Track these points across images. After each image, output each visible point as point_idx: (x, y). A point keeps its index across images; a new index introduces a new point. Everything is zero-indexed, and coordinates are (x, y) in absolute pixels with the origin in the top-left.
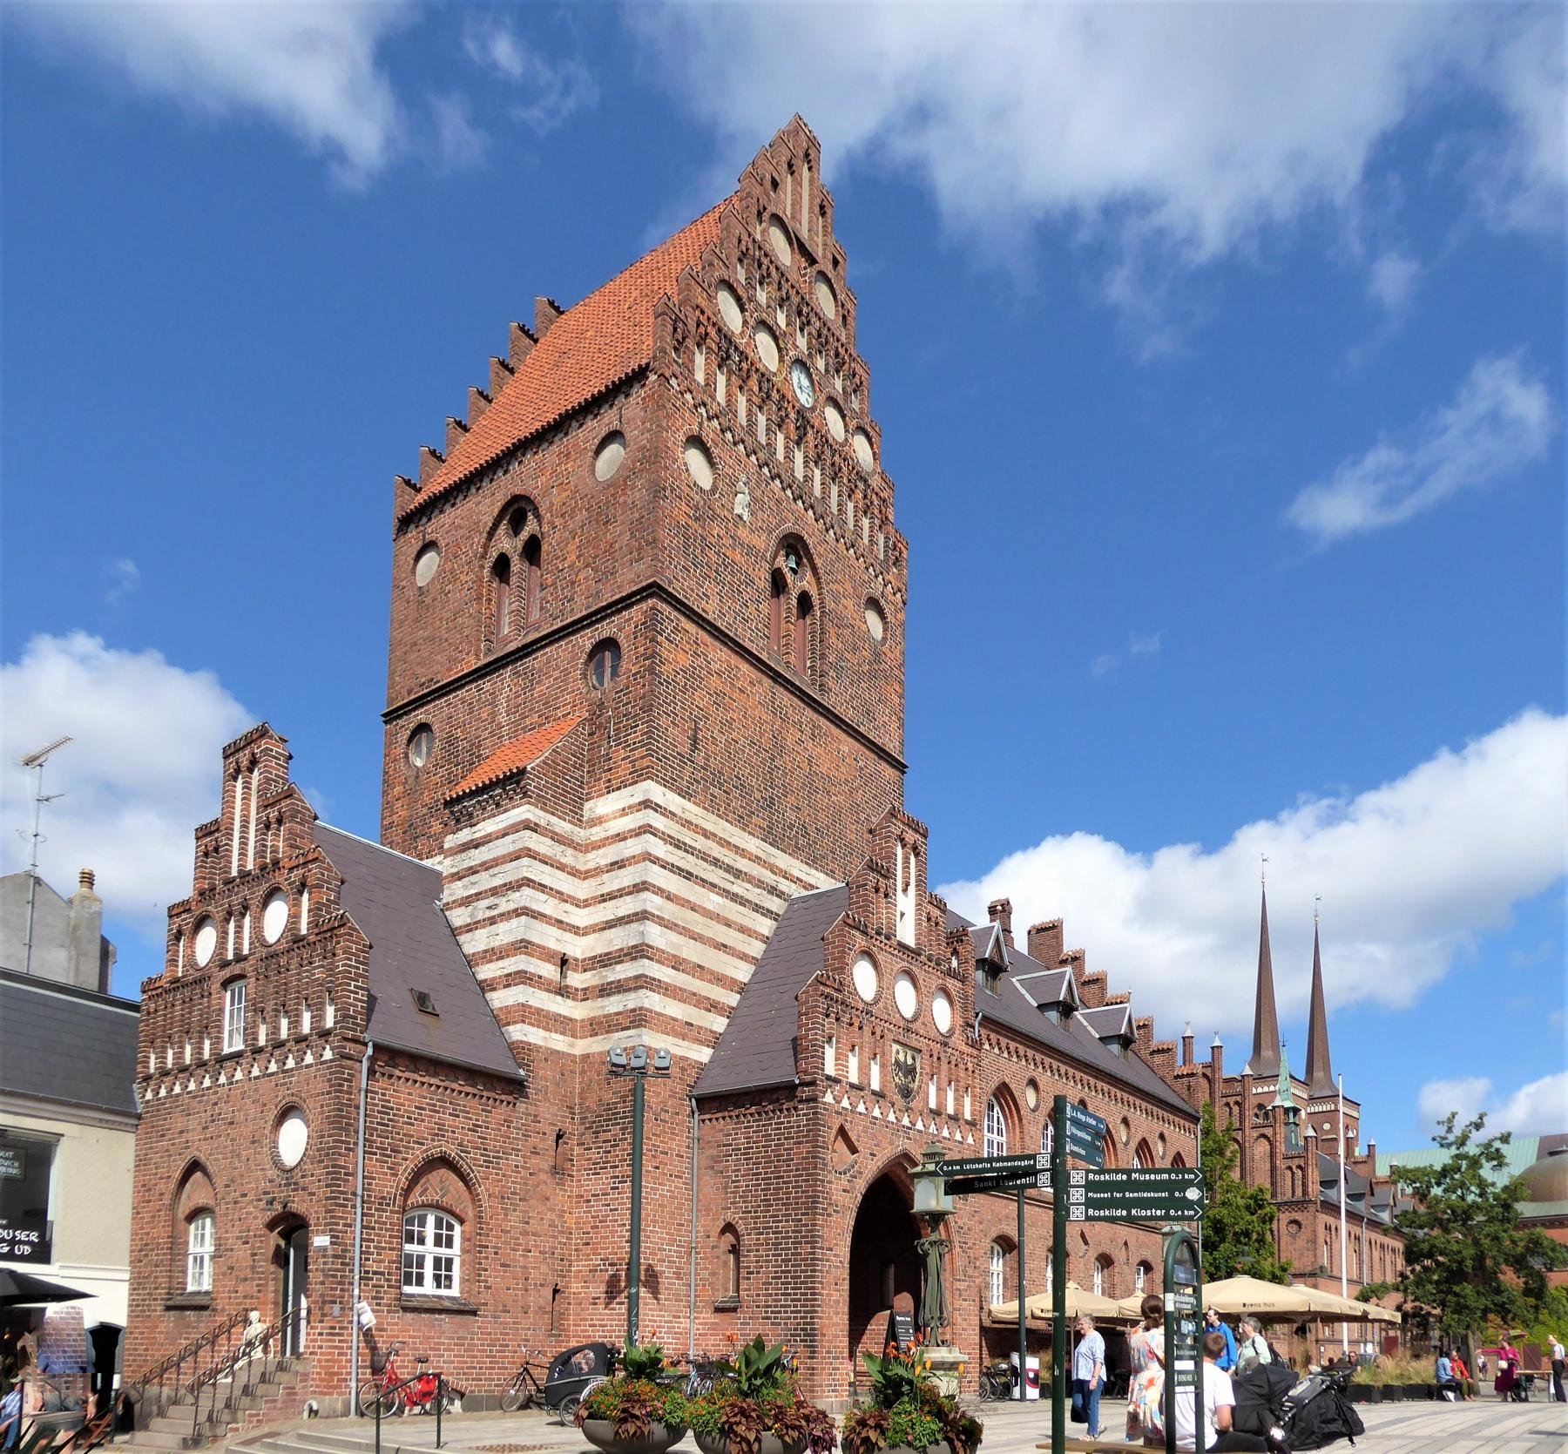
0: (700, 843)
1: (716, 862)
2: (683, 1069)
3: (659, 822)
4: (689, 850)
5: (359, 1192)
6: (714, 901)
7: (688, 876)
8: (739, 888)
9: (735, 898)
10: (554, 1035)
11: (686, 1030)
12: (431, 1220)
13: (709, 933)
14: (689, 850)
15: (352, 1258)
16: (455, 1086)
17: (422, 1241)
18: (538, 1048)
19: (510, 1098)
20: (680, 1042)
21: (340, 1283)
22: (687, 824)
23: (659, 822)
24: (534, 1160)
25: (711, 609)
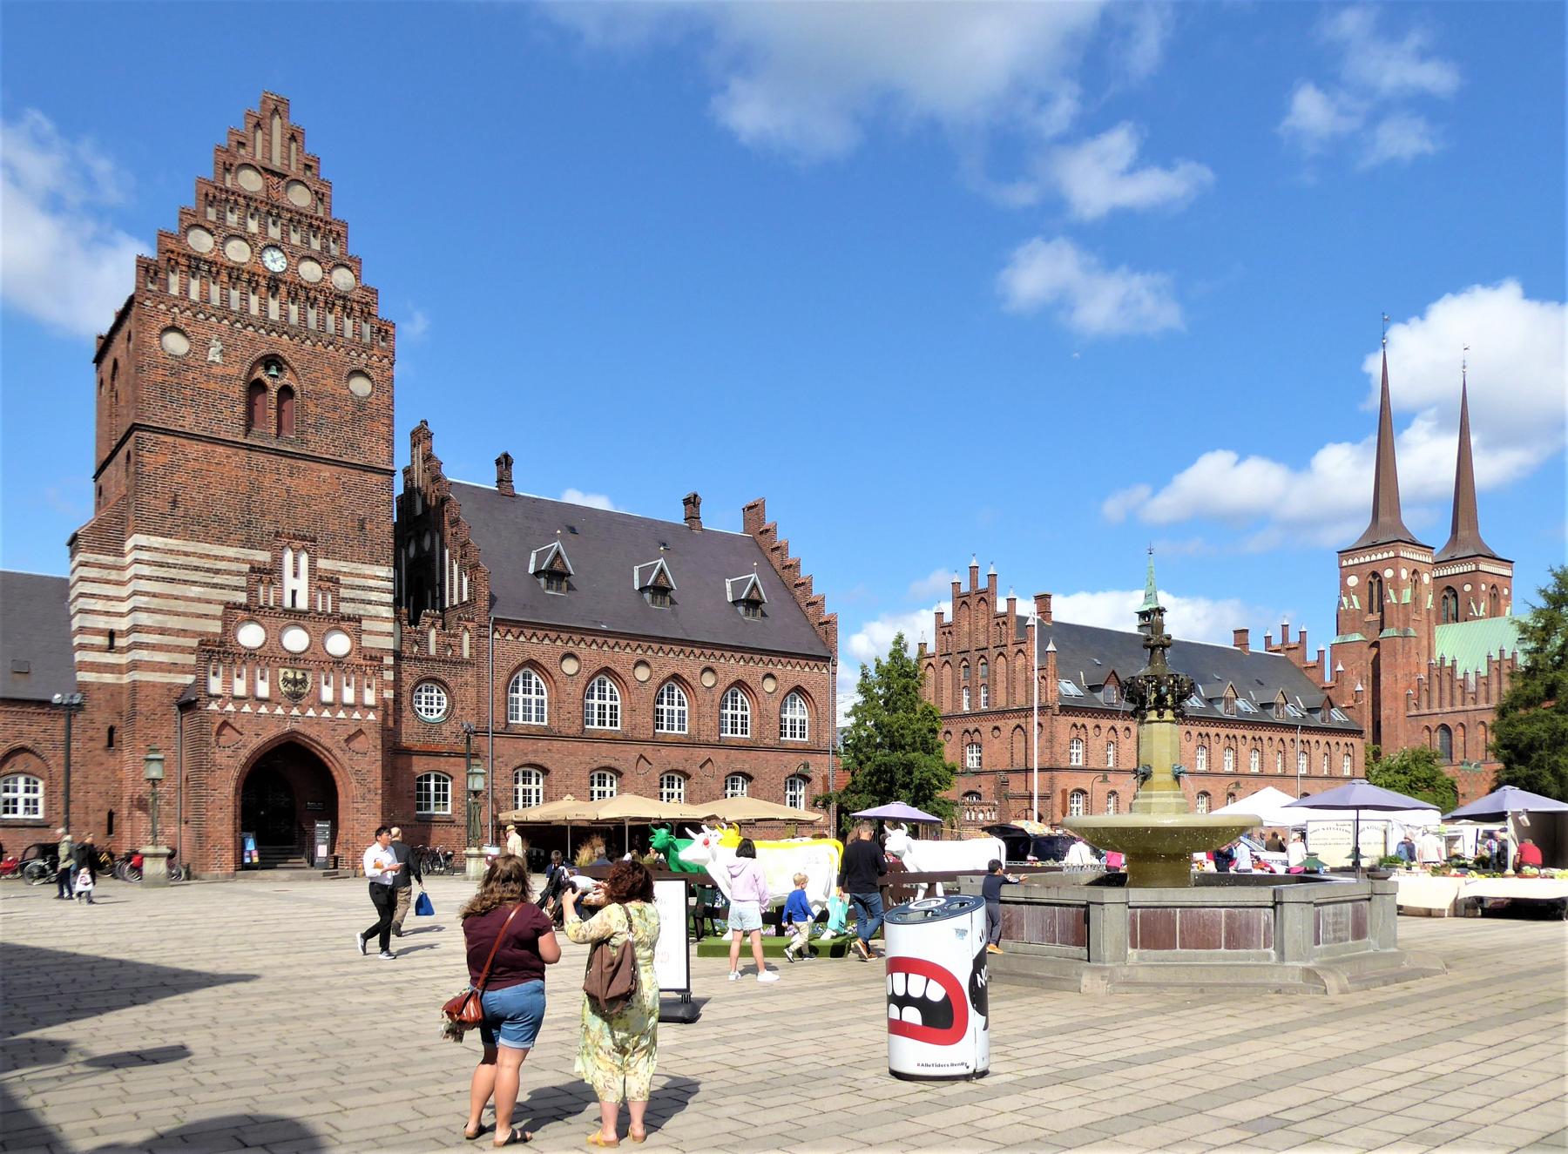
0: (182, 560)
1: (196, 569)
3: (145, 556)
4: (169, 566)
6: (195, 591)
8: (218, 579)
9: (215, 586)
11: (172, 668)
13: (192, 610)
14: (169, 566)
18: (92, 684)
22: (171, 552)
23: (145, 556)
25: (188, 424)
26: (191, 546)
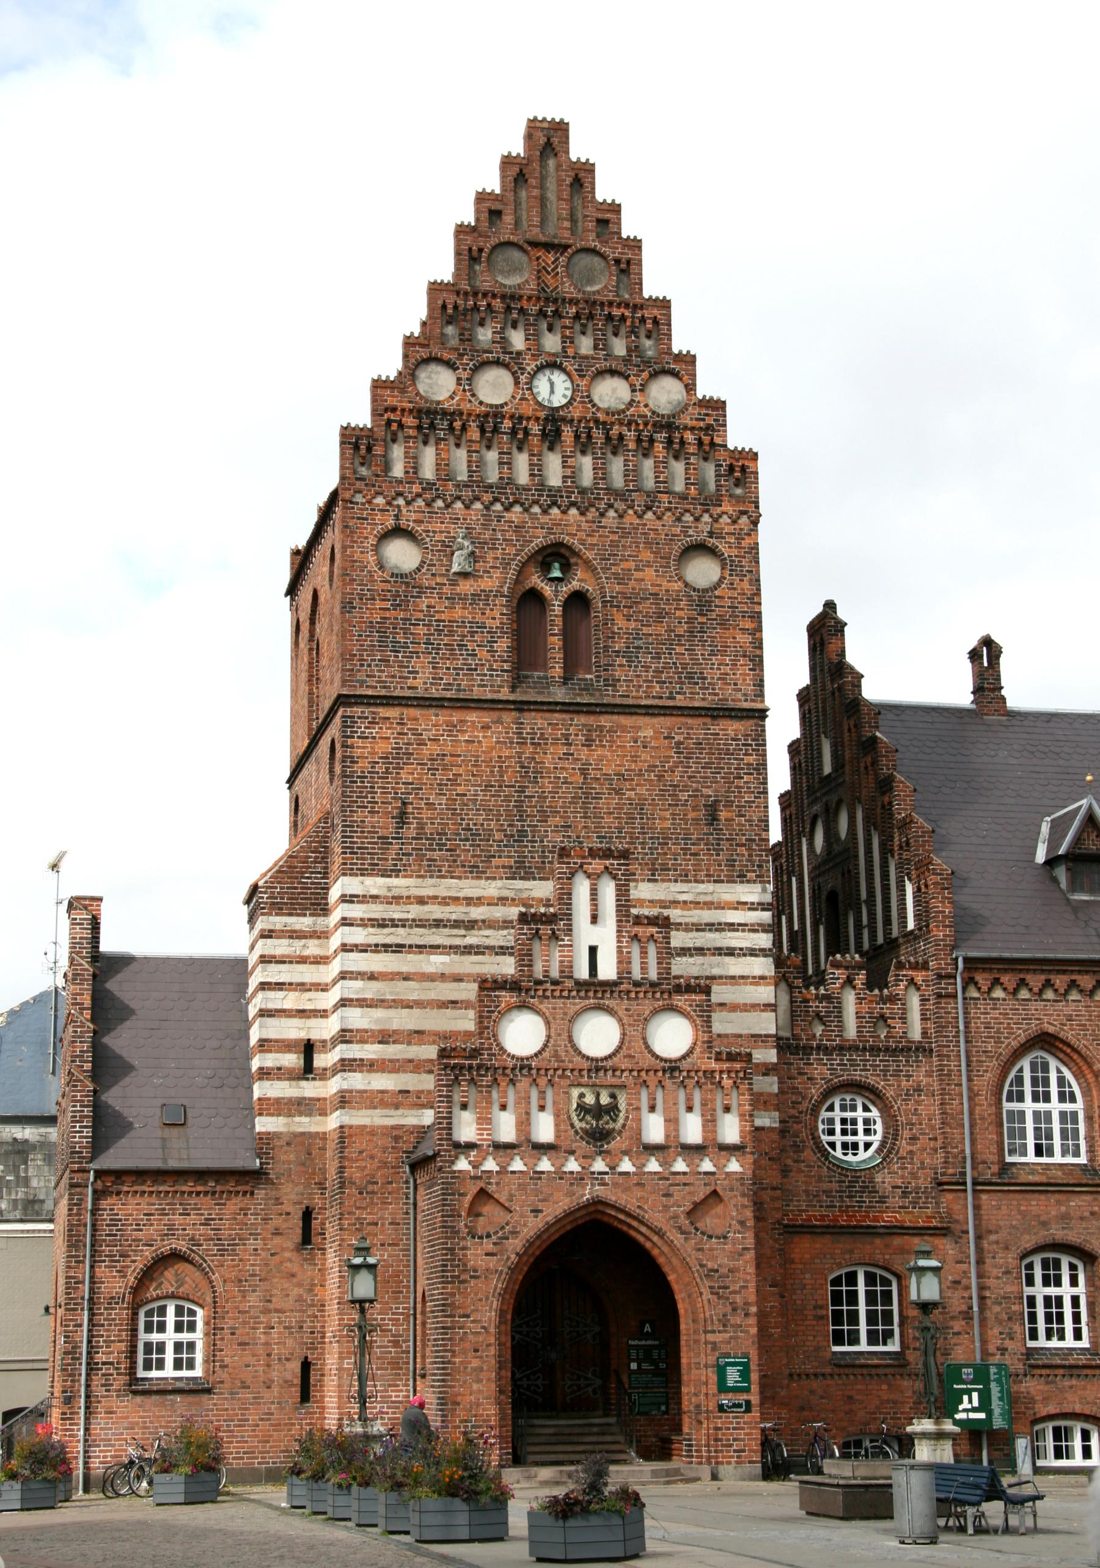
2: (397, 1138)
5: (87, 1297)
7: (398, 948)
10: (297, 1119)
12: (171, 1311)
15: (81, 1354)
16: (185, 1188)
17: (162, 1328)
19: (247, 1188)
20: (392, 1112)
21: (70, 1375)
24: (277, 1240)
26: (428, 887)
